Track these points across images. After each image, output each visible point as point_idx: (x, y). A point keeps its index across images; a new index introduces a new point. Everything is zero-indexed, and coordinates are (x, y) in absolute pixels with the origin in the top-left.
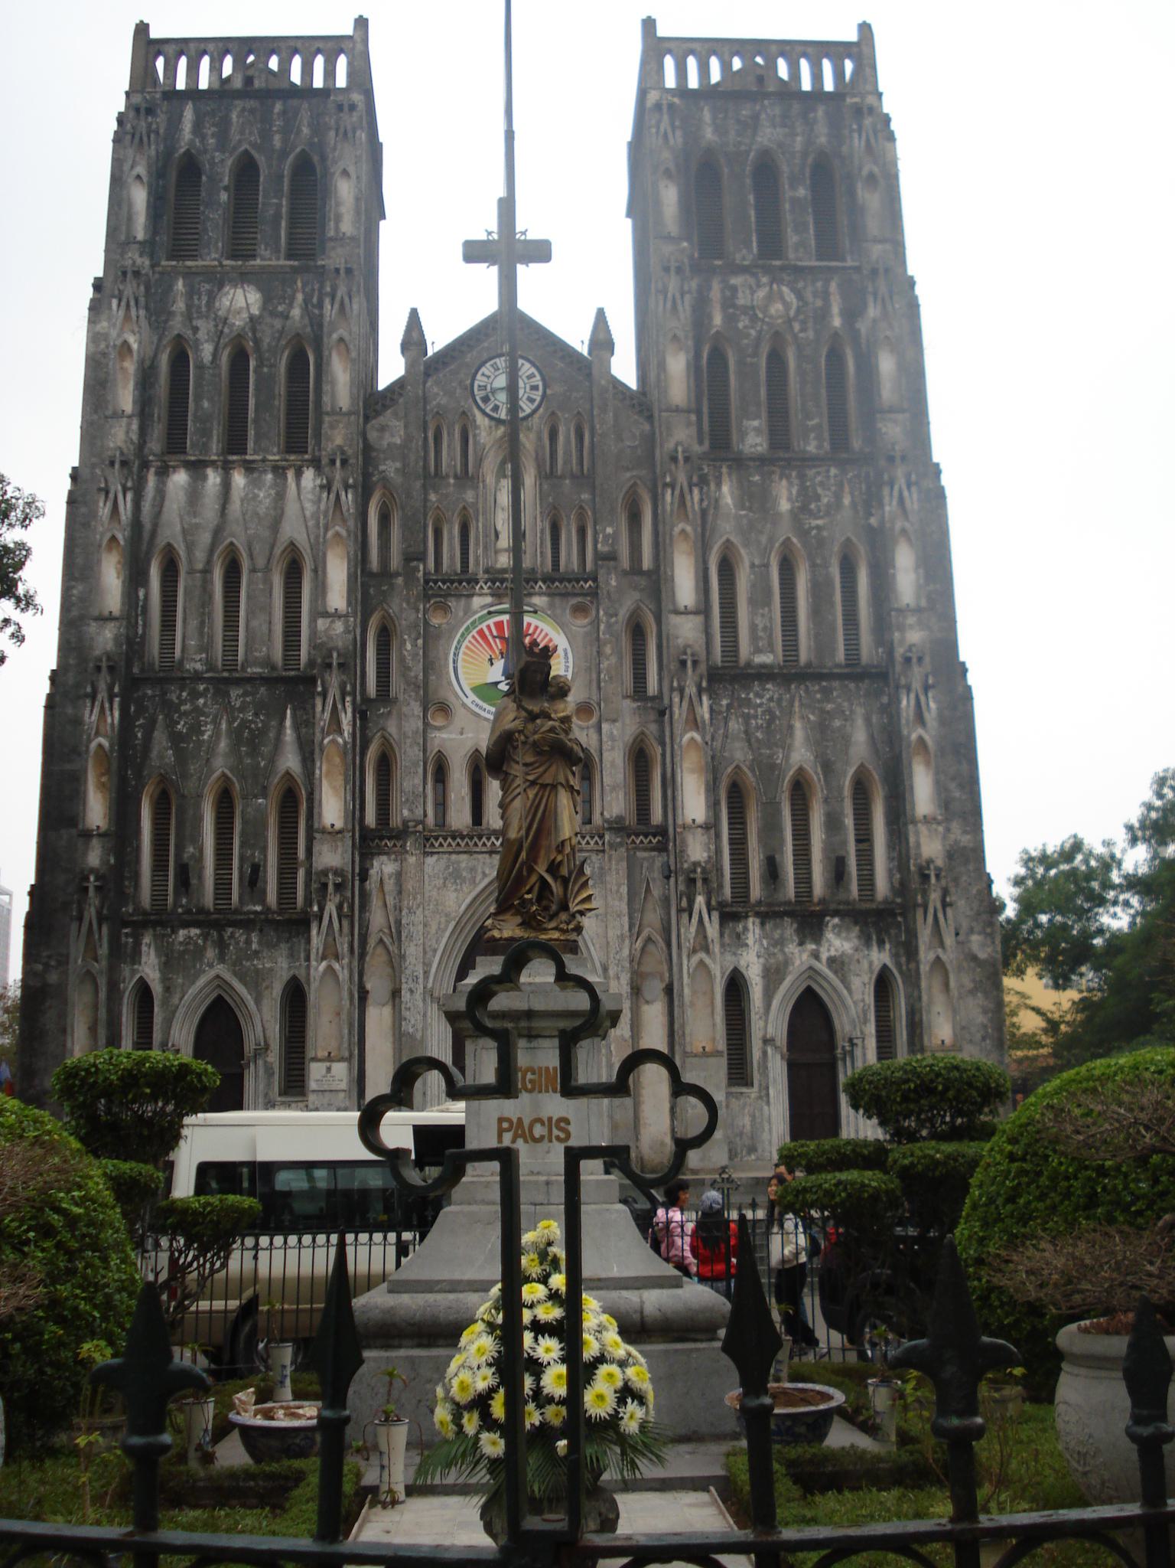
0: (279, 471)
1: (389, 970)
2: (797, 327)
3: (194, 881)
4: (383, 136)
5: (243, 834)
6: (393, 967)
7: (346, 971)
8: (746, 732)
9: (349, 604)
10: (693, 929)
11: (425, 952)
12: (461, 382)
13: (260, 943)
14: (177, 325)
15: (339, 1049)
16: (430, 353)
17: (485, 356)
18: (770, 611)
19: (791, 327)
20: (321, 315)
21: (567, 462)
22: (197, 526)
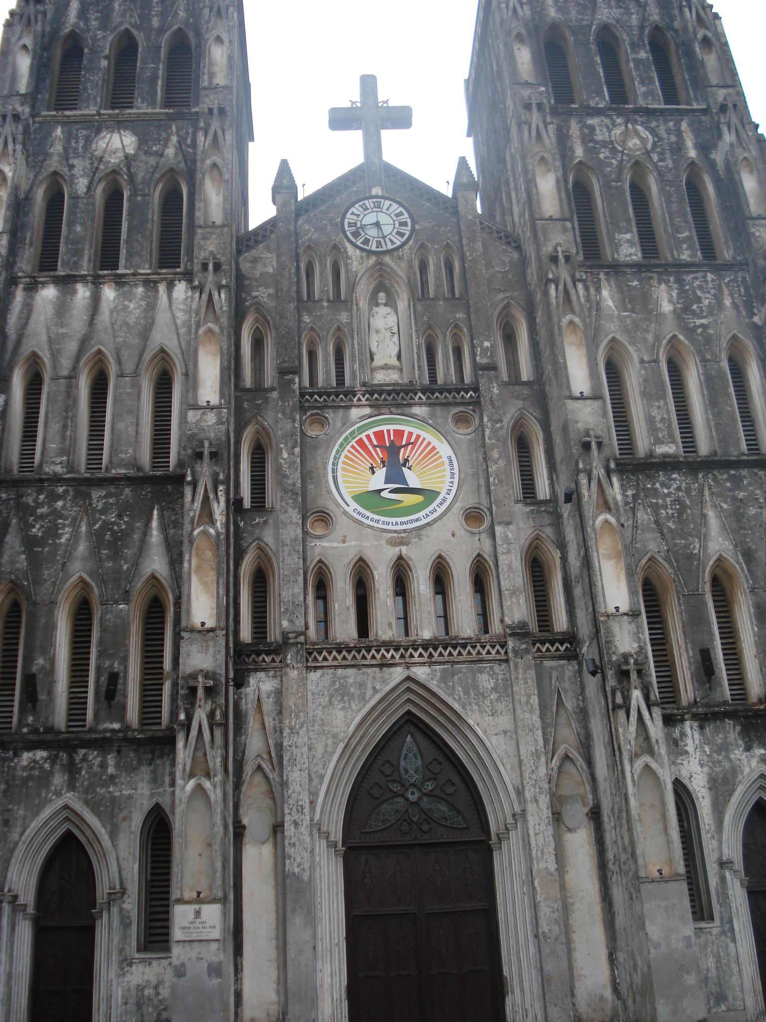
0: (150, 284)
1: (268, 802)
2: (655, 157)
3: (42, 697)
4: (252, 80)
5: (101, 642)
6: (273, 799)
7: (219, 792)
8: (657, 522)
9: (222, 396)
10: (633, 728)
11: (311, 780)
12: (331, 221)
13: (117, 766)
14: (54, 164)
15: (211, 888)
16: (300, 197)
17: (354, 198)
18: (666, 403)
19: (651, 159)
20: (195, 154)
21: (438, 286)
22: (64, 336)
